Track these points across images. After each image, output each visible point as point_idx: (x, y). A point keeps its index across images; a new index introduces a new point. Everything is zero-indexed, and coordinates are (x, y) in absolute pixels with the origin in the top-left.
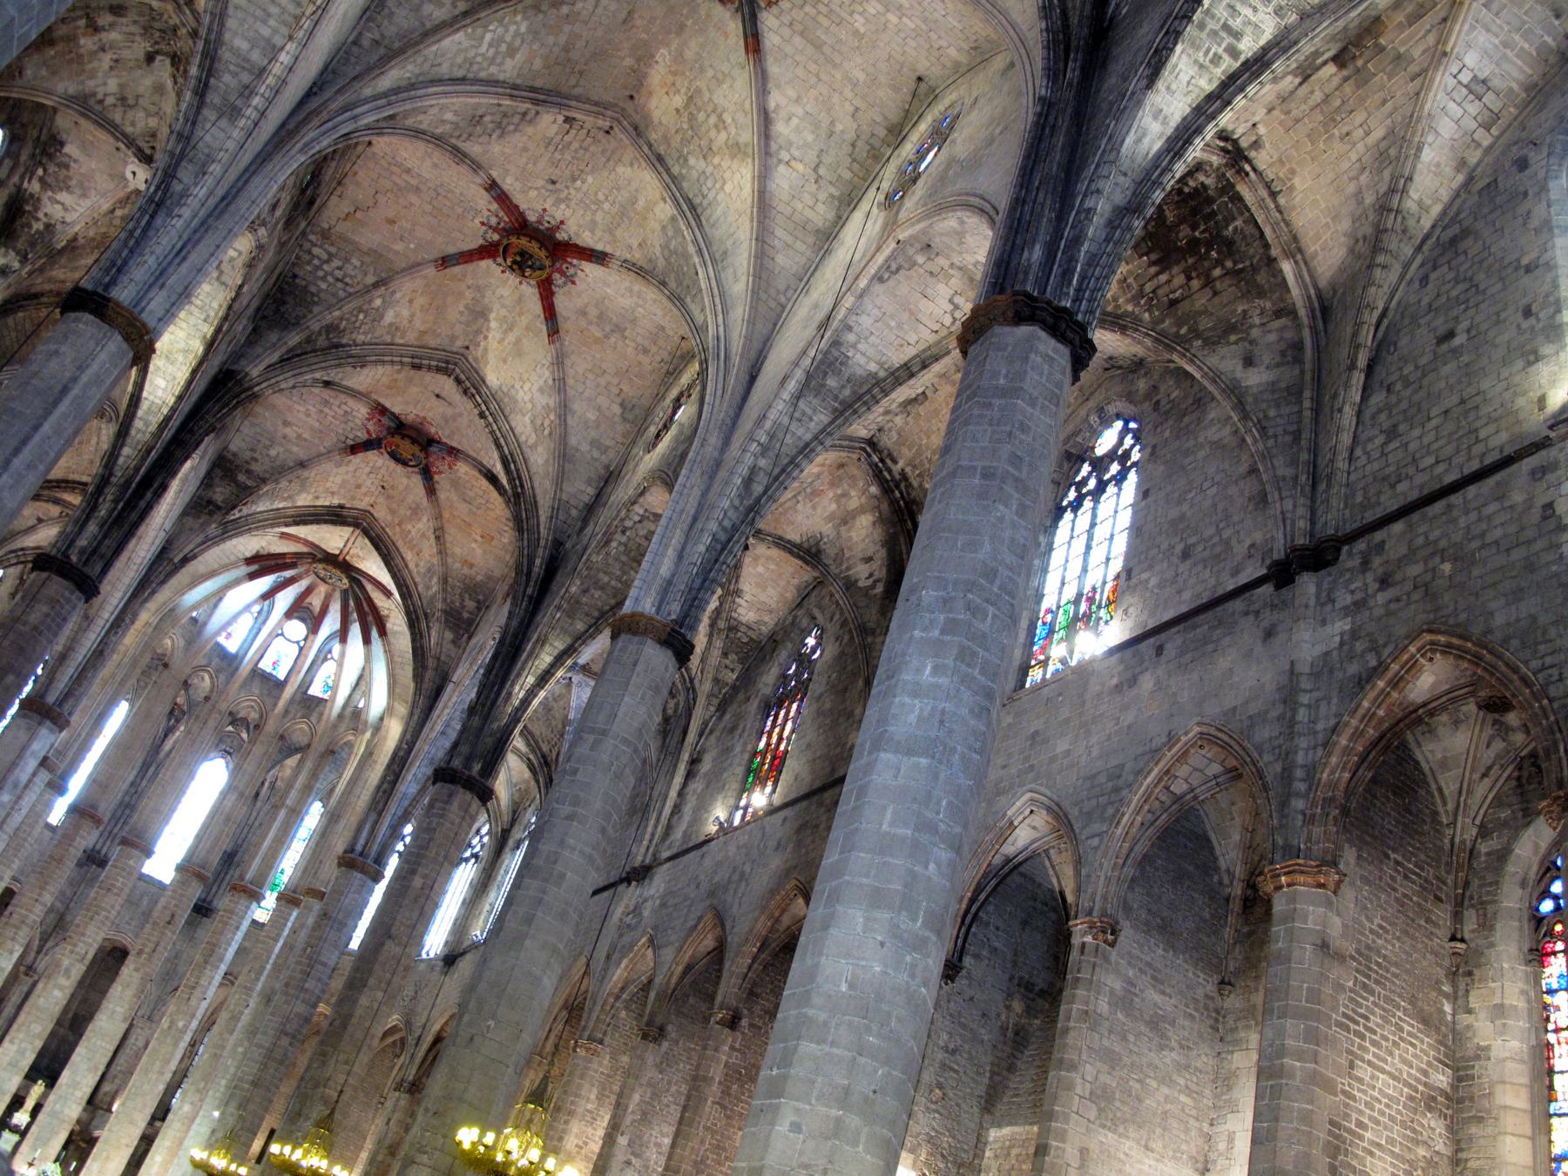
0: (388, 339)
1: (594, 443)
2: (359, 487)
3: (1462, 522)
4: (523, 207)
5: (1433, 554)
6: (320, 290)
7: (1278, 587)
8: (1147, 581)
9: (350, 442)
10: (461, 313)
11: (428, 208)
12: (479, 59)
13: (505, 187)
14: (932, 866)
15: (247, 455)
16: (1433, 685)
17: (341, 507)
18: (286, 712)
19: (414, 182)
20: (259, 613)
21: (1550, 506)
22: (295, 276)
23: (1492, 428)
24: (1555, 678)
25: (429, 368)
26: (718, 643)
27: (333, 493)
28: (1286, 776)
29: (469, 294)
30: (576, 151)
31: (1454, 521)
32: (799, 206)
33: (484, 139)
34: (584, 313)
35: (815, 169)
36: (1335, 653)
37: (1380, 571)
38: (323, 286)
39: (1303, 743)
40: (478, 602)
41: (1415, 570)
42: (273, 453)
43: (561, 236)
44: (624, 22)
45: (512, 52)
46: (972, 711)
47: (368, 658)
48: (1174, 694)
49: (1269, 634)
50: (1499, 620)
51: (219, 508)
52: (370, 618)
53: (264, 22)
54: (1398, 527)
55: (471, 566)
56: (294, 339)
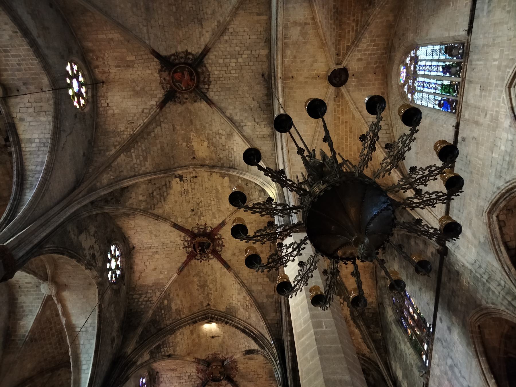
1: (268, 297)
4: (190, 229)
6: (142, 309)
10: (198, 290)
11: (163, 256)
12: (136, 166)
13: (180, 224)
19: (154, 250)
22: (131, 310)
26: (361, 323)
29: (196, 279)
30: (192, 192)
32: (258, 133)
33: (160, 204)
34: (234, 254)
35: (255, 121)
38: (143, 307)
43: (208, 231)
44: (174, 130)
45: (145, 159)
53: (38, 158)
56: (140, 330)
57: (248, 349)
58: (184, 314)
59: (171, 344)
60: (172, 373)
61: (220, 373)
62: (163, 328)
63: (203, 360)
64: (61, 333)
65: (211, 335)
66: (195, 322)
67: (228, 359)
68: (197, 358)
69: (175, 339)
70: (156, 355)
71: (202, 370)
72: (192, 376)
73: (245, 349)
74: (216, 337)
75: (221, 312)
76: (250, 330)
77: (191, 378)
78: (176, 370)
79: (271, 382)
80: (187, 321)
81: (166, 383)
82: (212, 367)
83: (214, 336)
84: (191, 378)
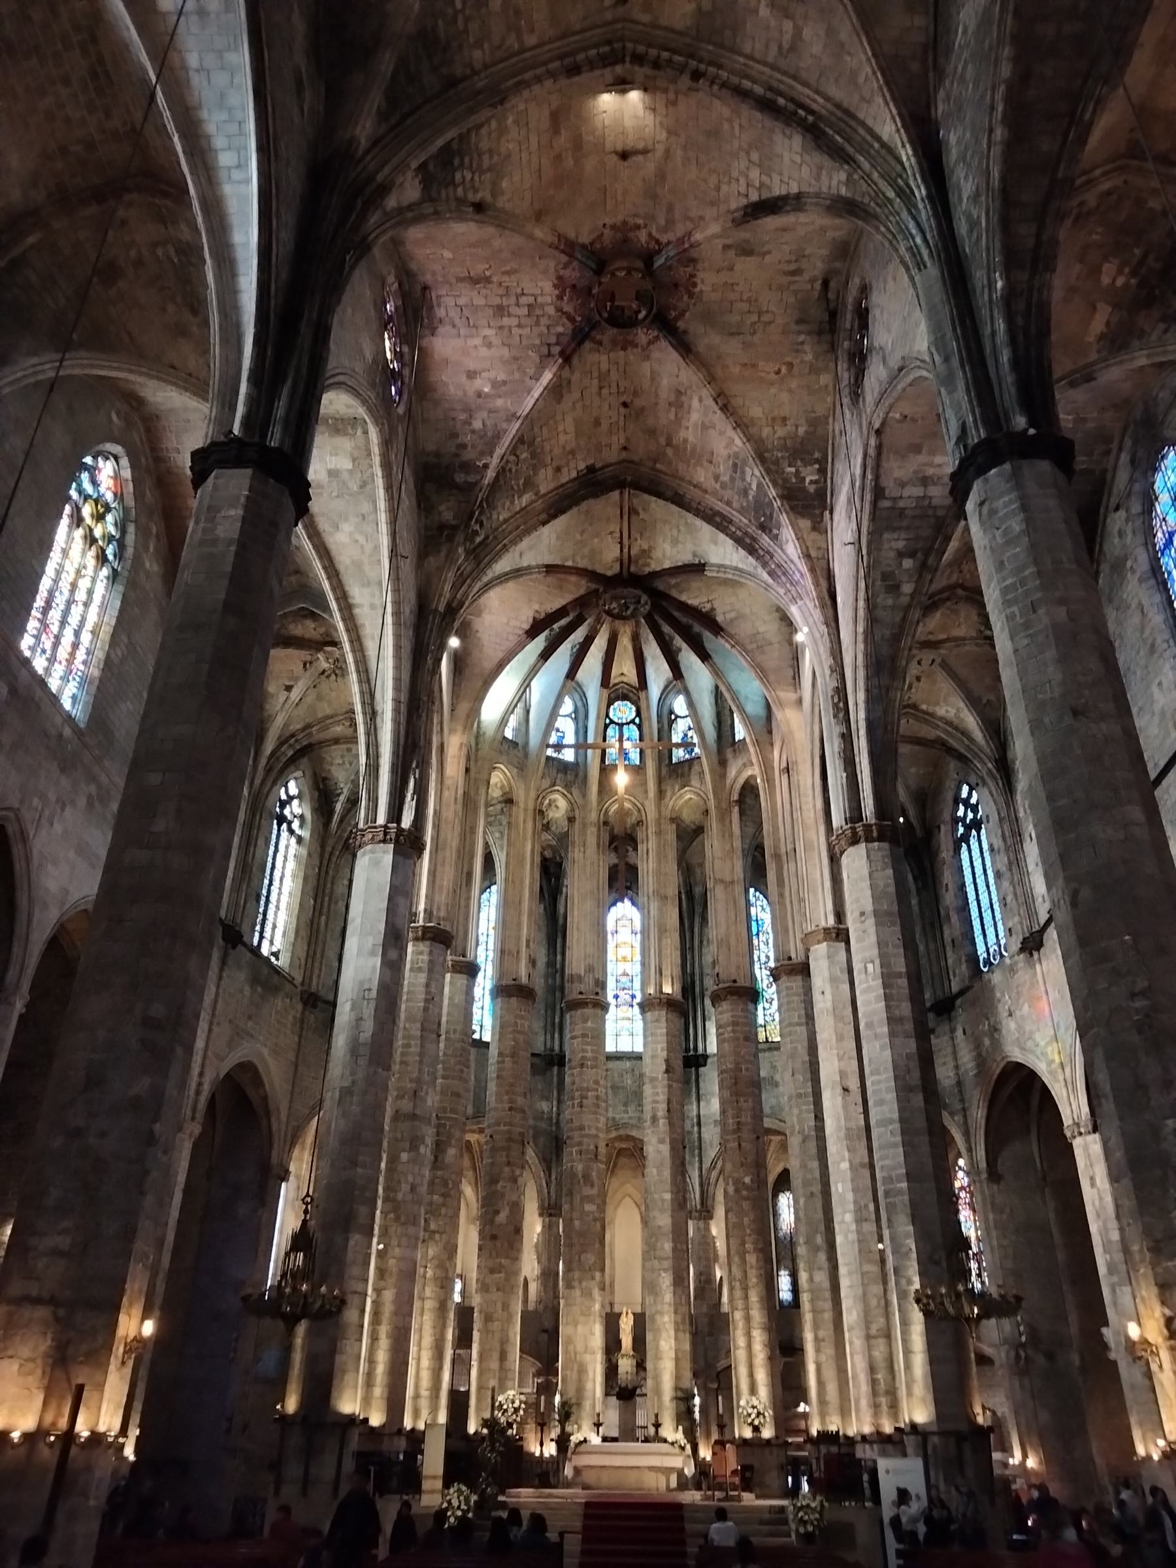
0: (512, 42)
2: (597, 423)
9: (556, 350)
15: (451, 447)
17: (591, 469)
18: (661, 794)
20: (576, 711)
25: (592, 65)
27: (572, 452)
40: (817, 461)
42: (477, 424)
47: (717, 672)
51: (455, 528)
52: (697, 628)
55: (784, 419)
56: (387, 62)
57: (754, 197)
58: (532, 31)
59: (486, 162)
60: (475, 293)
61: (638, 297)
62: (461, 81)
63: (584, 246)
64: (94, 39)
65: (619, 148)
66: (574, 70)
67: (670, 247)
68: (566, 239)
69: (499, 139)
70: (439, 193)
71: (574, 286)
72: (542, 306)
73: (744, 201)
74: (637, 152)
75: (673, 31)
76: (792, 100)
77: (538, 312)
78: (488, 280)
79: (802, 338)
80: (545, 63)
81: (454, 326)
82: (613, 274)
83: (628, 148)
84: (538, 312)
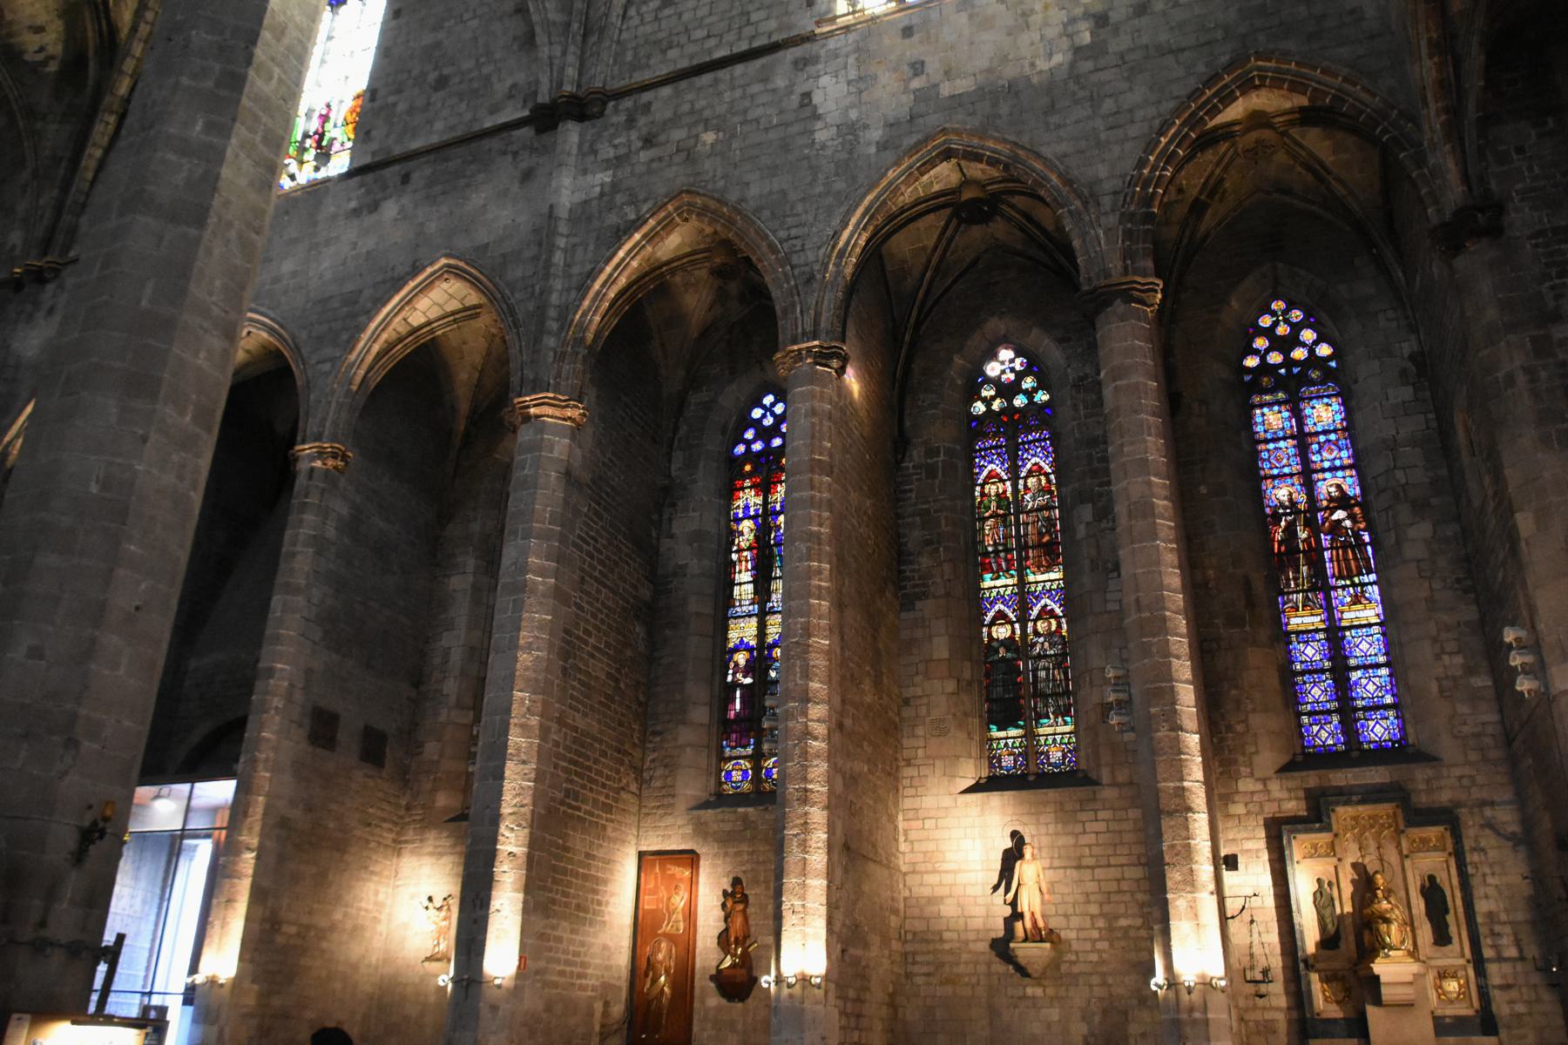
3: (727, 96)
5: (696, 123)
7: (539, 131)
8: (395, 105)
14: (202, 355)
16: (679, 247)
21: (807, 95)
23: (762, 14)
24: (798, 248)
28: (542, 309)
31: (720, 94)
36: (595, 203)
37: (645, 131)
39: (558, 284)
41: (678, 134)
46: (251, 184)
48: (422, 224)
49: (527, 176)
50: (754, 191)
54: (666, 91)
